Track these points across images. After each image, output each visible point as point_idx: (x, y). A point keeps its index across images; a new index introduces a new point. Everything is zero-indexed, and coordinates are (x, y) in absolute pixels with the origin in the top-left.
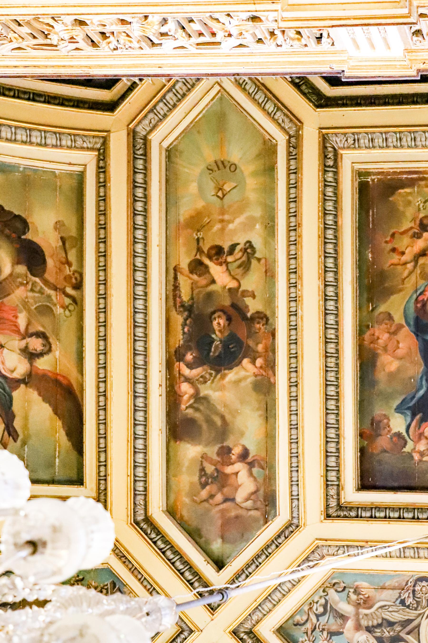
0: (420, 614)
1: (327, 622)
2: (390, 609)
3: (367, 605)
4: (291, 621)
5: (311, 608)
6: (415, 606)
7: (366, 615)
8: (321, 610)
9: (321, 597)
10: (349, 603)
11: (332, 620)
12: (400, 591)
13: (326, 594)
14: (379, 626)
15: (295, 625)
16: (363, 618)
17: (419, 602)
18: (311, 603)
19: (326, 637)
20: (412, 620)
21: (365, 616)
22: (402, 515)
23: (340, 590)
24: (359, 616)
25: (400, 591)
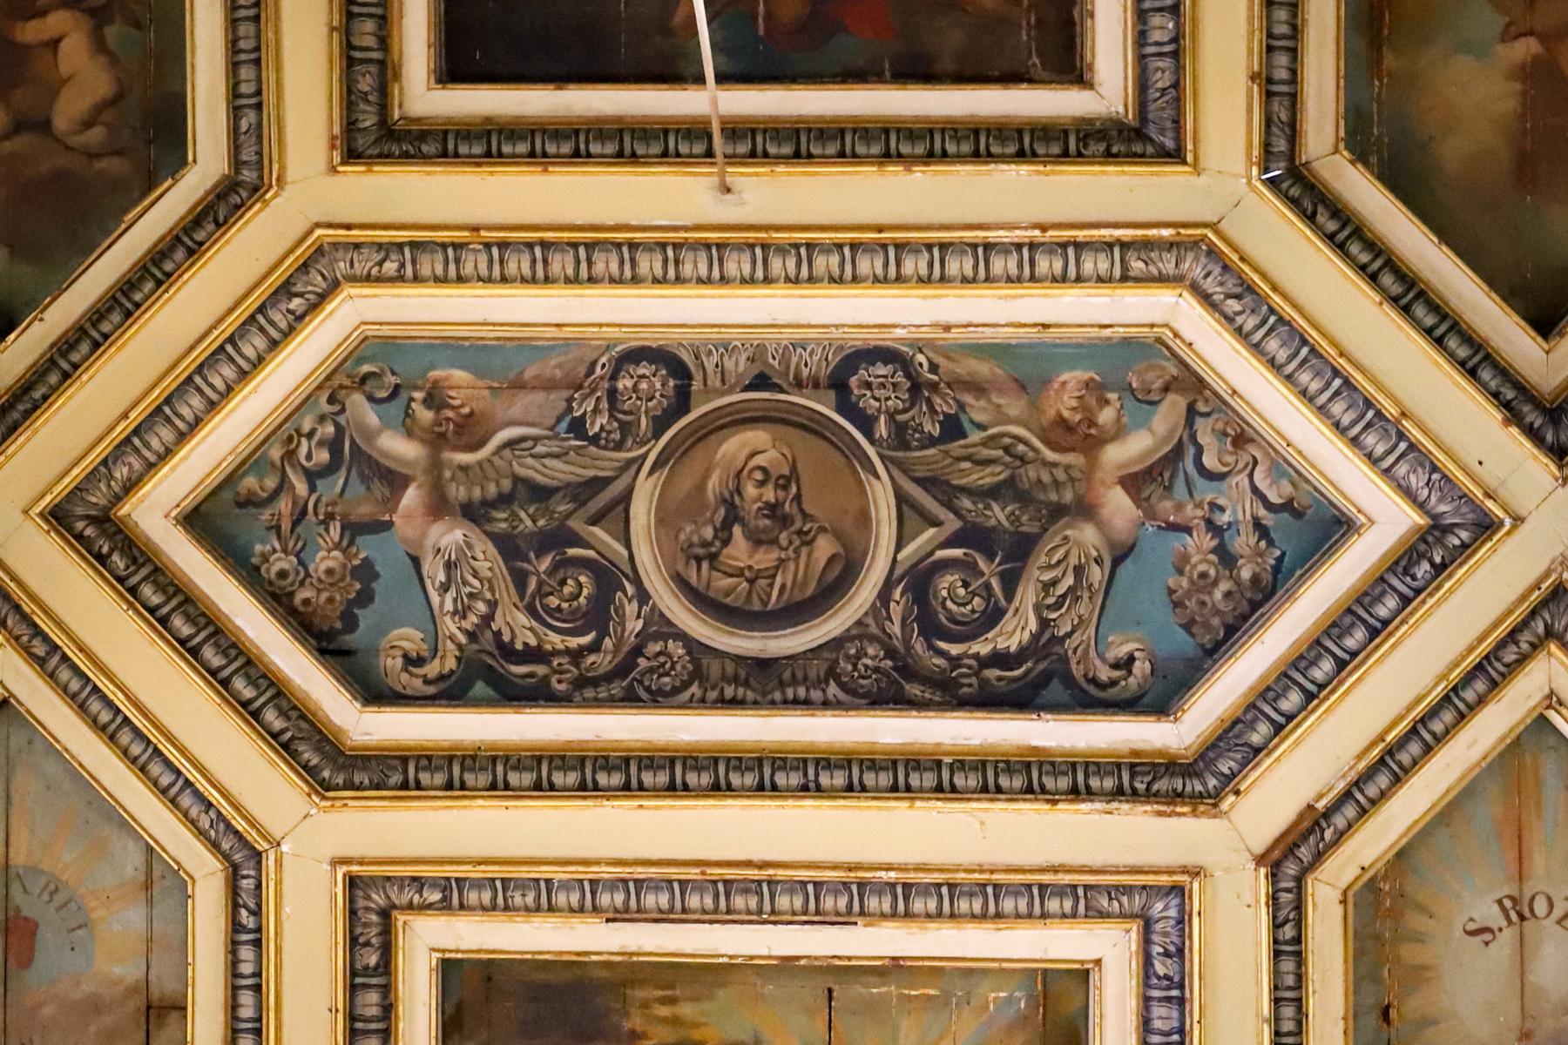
0: (633, 460)
1: (343, 491)
2: (540, 449)
3: (465, 440)
4: (227, 495)
5: (290, 455)
6: (617, 436)
7: (464, 469)
8: (323, 456)
9: (322, 419)
10: (410, 434)
11: (357, 488)
12: (566, 394)
13: (336, 408)
14: (504, 500)
15: (240, 505)
16: (453, 478)
17: (629, 423)
18: (290, 439)
19: (337, 539)
20: (607, 481)
21: (460, 474)
22: (582, 146)
23: (384, 394)
24: (440, 476)
25: (566, 394)
